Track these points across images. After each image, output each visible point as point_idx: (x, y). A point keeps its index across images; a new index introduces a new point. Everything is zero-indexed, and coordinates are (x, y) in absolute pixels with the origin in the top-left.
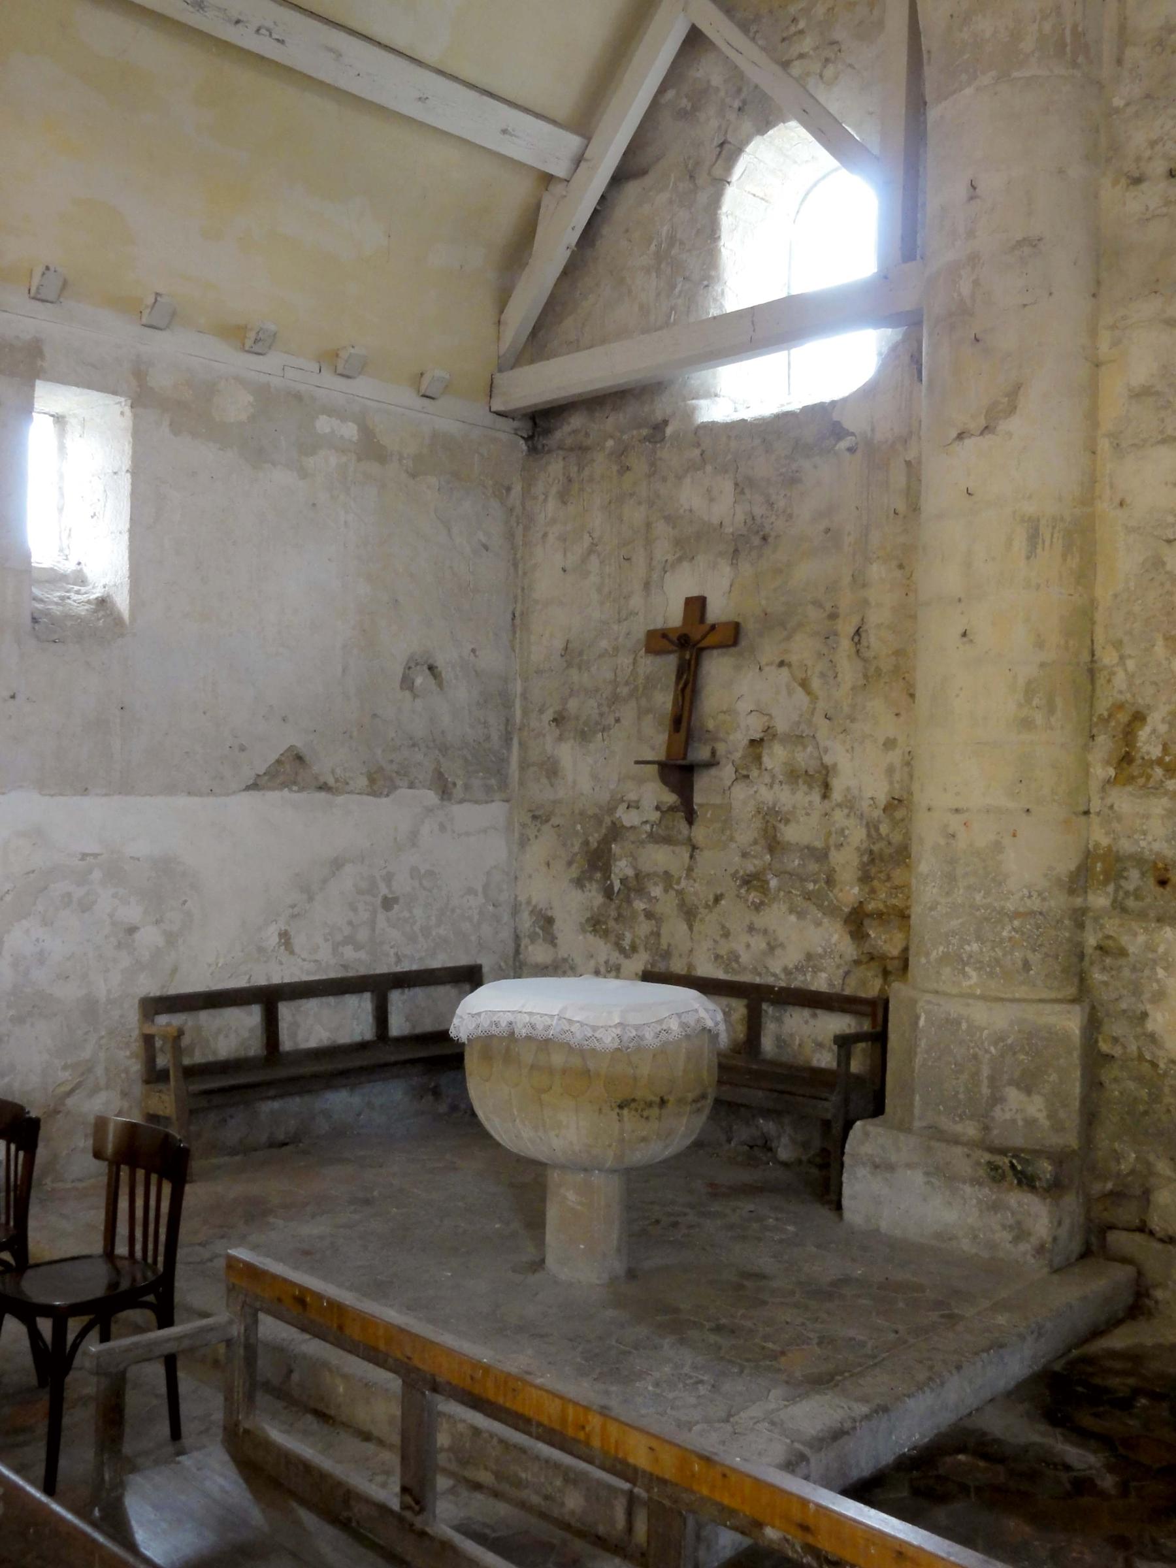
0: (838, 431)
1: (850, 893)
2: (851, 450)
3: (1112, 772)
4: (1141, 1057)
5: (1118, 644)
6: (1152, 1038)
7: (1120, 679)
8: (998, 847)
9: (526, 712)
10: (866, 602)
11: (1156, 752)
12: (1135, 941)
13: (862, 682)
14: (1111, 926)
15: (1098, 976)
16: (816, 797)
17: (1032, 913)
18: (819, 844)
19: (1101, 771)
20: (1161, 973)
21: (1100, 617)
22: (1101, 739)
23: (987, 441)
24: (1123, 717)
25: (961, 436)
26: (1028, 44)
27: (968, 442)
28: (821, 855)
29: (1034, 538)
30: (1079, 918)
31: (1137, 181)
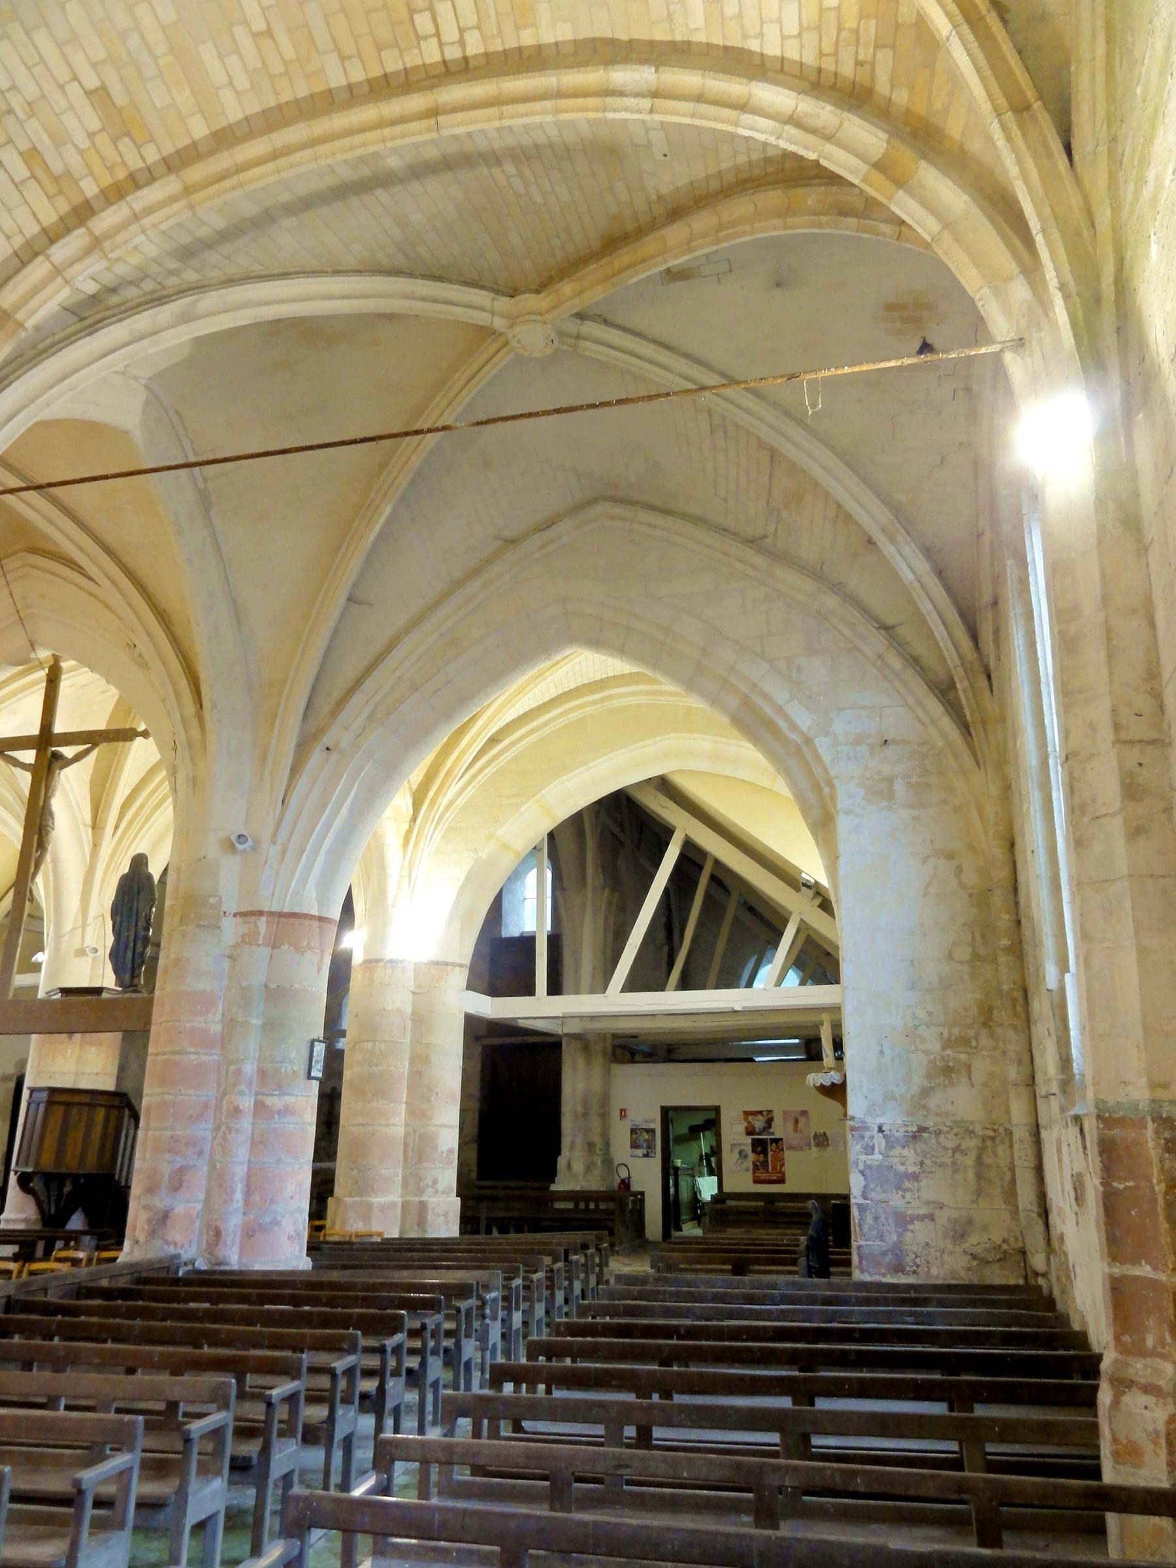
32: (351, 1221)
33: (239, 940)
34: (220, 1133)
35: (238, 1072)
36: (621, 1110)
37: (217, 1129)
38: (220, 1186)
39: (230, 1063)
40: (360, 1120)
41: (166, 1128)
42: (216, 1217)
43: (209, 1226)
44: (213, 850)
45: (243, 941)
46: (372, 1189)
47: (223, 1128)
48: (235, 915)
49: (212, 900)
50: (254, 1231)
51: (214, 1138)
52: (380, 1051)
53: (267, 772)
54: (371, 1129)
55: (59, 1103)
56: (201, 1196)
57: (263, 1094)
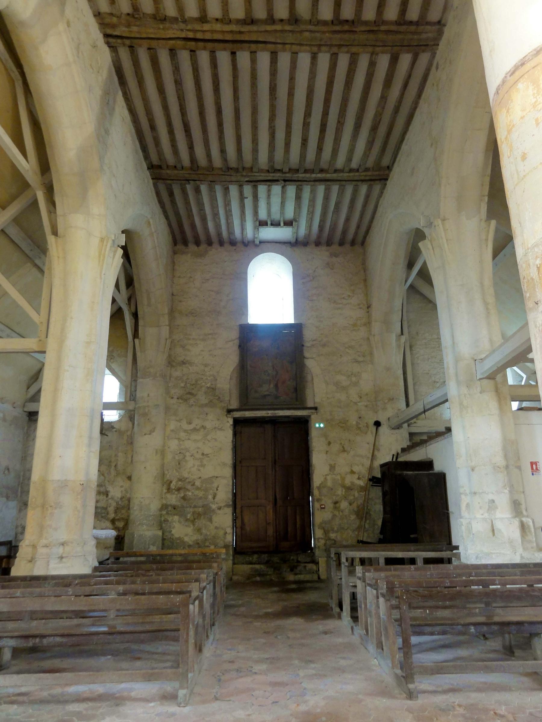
0: (113, 427)
1: (112, 516)
2: (116, 431)
3: (166, 491)
4: (170, 538)
5: (168, 470)
6: (173, 535)
7: (168, 476)
8: (149, 504)
9: (23, 480)
10: (117, 460)
11: (174, 488)
12: (170, 519)
13: (116, 475)
14: (166, 517)
15: (164, 525)
16: (105, 497)
17: (155, 515)
18: (105, 506)
19: (165, 491)
20: (174, 523)
21: (165, 465)
22: (165, 485)
23: (149, 436)
24: (168, 482)
25: (145, 434)
26: (158, 375)
27: (147, 436)
28: (106, 509)
29: (157, 452)
30: (161, 515)
31: (172, 398)
36: (532, 464)
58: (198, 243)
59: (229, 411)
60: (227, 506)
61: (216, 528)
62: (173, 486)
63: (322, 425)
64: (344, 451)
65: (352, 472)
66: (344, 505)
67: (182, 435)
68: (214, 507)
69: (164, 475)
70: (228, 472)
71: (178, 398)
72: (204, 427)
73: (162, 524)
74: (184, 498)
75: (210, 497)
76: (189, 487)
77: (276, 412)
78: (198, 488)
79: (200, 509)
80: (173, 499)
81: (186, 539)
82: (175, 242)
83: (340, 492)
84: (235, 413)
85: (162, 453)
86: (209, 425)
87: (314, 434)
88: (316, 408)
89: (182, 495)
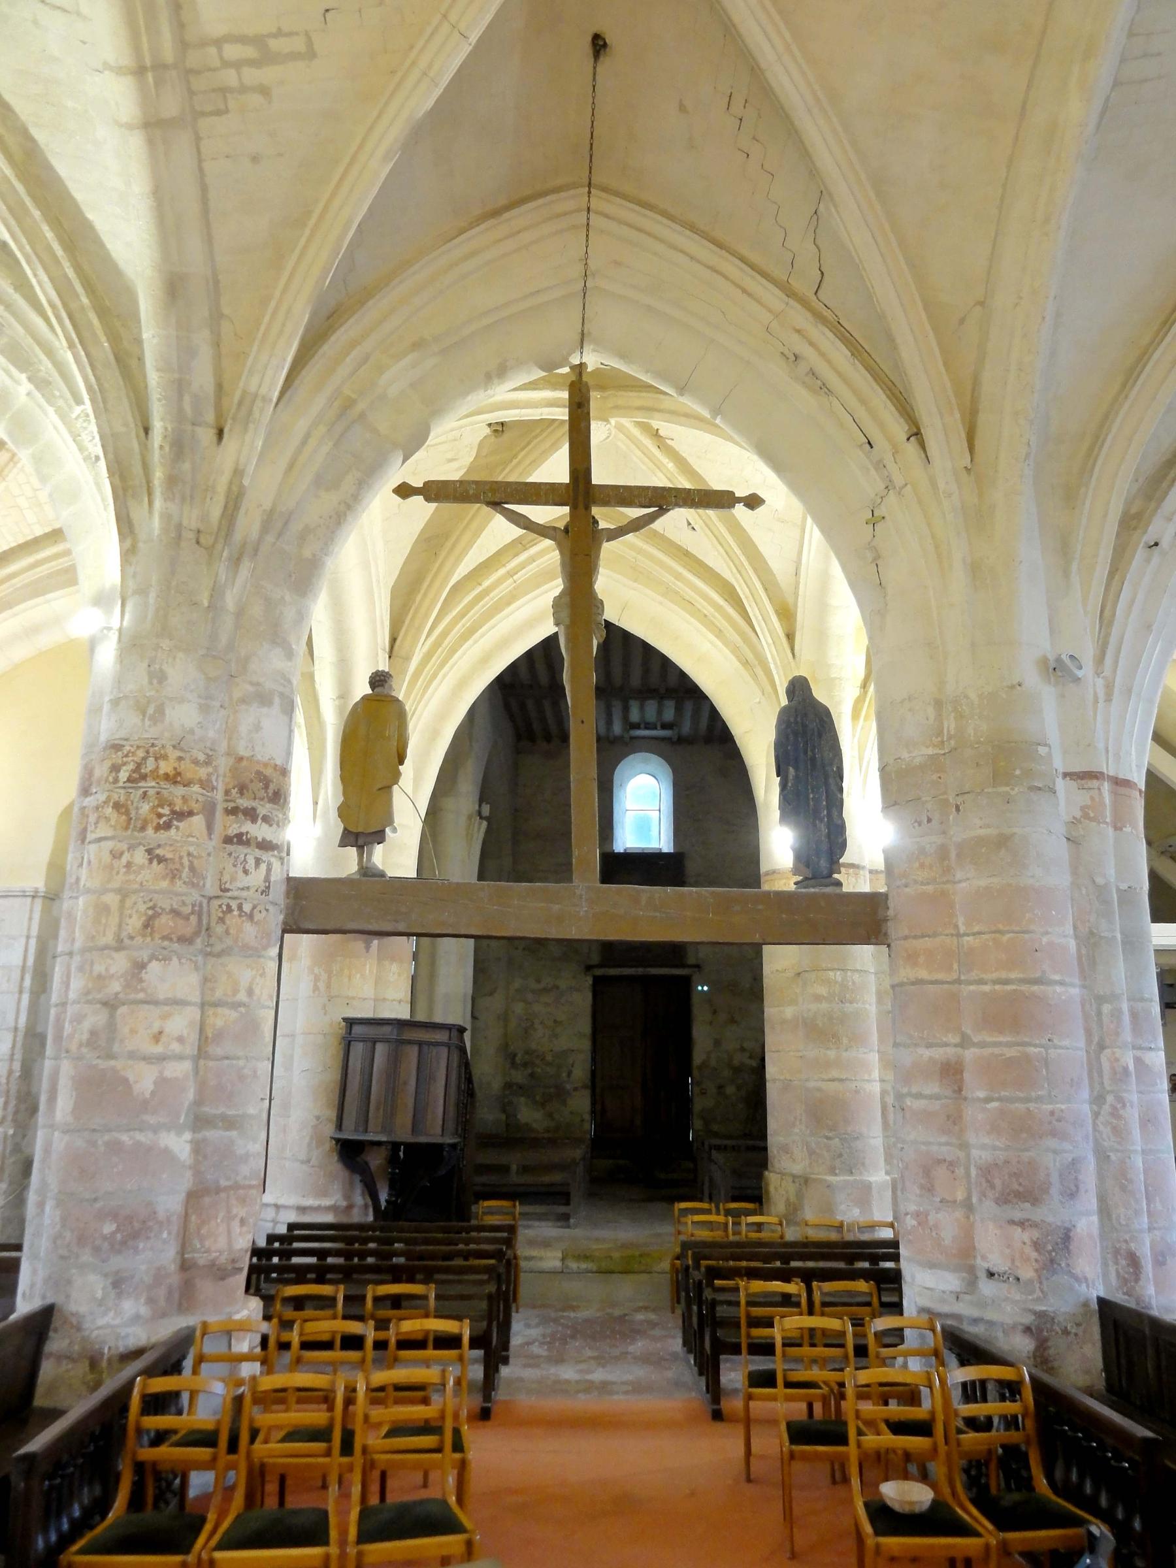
31: (517, 949)
32: (843, 1207)
33: (1078, 814)
34: (1106, 1108)
35: (1117, 1014)
37: (1098, 1099)
38: (1123, 1188)
39: (1101, 999)
40: (834, 1073)
41: (1039, 1099)
42: (1127, 1237)
43: (1117, 1252)
44: (1032, 678)
45: (1086, 816)
46: (863, 1164)
47: (1110, 1099)
48: (1065, 775)
49: (1042, 750)
50: (1164, 1256)
51: (1096, 1115)
52: (854, 983)
53: (1074, 566)
54: (852, 1086)
55: (410, 1042)
56: (1094, 1204)
57: (1140, 1048)
58: (548, 738)
59: (589, 968)
60: (585, 1087)
61: (571, 1113)
62: (518, 1059)
63: (706, 988)
64: (733, 1021)
65: (743, 1049)
66: (730, 1090)
67: (530, 996)
68: (568, 1087)
69: (507, 1045)
70: (586, 1045)
71: (524, 949)
72: (557, 987)
73: (506, 1107)
74: (532, 1075)
75: (564, 1075)
76: (538, 1062)
77: (649, 969)
78: (549, 1064)
79: (552, 1090)
80: (519, 1077)
81: (535, 1125)
82: (518, 737)
83: (727, 1073)
84: (595, 970)
85: (504, 1018)
86: (563, 984)
87: (695, 1001)
88: (698, 966)
89: (530, 1071)
